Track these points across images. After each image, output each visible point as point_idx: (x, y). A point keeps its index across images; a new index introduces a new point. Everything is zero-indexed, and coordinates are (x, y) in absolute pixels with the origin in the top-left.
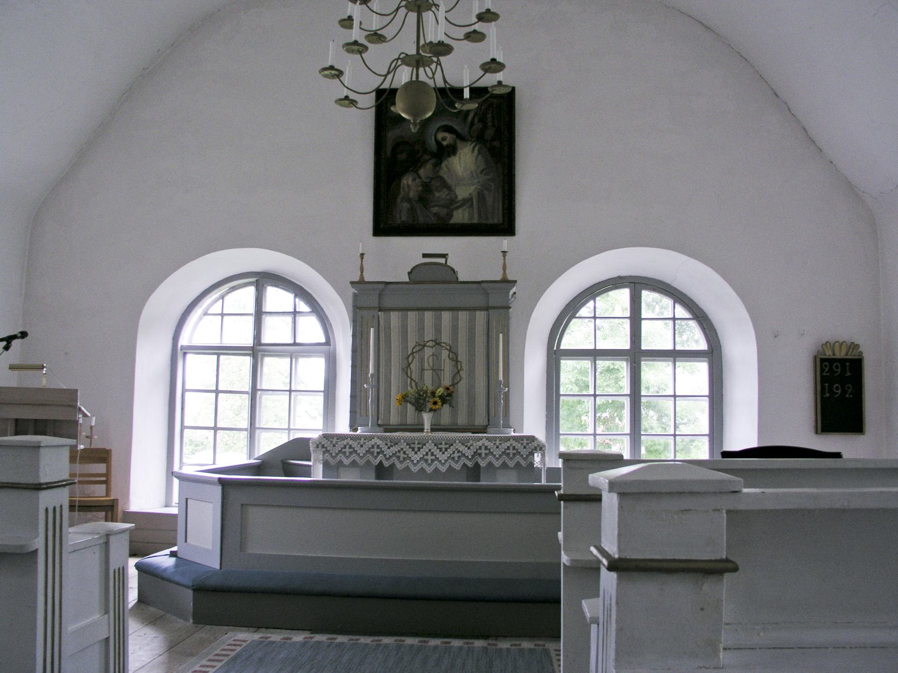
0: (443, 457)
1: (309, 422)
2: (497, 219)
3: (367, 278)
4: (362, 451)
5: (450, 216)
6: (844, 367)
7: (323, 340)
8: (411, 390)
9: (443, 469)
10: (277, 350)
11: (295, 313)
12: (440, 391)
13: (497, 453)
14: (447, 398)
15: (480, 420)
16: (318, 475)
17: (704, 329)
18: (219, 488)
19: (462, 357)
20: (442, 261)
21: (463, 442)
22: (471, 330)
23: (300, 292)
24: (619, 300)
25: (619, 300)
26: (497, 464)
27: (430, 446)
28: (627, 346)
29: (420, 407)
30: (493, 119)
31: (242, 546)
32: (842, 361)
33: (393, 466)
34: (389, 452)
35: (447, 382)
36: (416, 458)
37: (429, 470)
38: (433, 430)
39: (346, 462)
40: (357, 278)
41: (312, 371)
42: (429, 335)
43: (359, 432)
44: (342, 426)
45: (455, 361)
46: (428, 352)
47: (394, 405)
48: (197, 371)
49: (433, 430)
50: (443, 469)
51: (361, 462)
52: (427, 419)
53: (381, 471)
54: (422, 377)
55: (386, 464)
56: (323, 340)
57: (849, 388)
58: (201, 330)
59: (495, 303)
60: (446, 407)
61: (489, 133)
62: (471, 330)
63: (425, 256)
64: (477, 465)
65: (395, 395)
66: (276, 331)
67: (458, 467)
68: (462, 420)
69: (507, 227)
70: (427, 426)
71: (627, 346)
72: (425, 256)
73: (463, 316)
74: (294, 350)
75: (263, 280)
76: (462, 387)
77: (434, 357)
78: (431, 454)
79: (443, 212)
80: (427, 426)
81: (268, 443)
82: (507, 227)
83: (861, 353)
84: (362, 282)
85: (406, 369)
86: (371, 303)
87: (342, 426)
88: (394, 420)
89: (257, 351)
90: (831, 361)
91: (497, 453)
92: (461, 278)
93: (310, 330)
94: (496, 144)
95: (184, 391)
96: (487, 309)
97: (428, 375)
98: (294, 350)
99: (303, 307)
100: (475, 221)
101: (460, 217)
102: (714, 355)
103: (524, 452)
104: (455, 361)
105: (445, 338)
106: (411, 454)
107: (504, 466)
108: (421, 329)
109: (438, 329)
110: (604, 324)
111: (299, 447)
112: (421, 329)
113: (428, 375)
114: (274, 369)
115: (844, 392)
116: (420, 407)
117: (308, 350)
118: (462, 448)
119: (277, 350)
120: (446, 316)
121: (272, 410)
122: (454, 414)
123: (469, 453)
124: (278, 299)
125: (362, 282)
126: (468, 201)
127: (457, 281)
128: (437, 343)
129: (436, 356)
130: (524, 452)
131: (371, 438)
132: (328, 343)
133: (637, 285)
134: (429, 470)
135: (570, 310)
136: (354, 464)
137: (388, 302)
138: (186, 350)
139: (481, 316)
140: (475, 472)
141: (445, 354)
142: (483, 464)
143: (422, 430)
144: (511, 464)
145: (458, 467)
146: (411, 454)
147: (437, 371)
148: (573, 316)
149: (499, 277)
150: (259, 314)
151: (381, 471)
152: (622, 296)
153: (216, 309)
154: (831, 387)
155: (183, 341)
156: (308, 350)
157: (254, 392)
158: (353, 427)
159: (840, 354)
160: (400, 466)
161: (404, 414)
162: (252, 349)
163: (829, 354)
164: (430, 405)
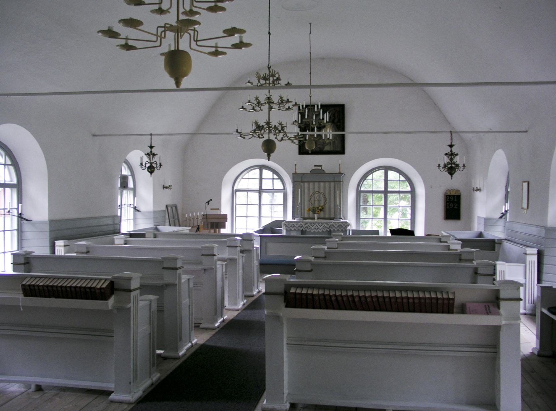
0: (320, 228)
1: (278, 214)
2: (339, 149)
3: (298, 172)
4: (297, 226)
5: (324, 148)
6: (454, 198)
7: (283, 188)
8: (311, 207)
9: (320, 231)
10: (267, 191)
11: (273, 179)
12: (320, 208)
13: (336, 227)
14: (322, 209)
15: (332, 216)
16: (284, 233)
17: (409, 184)
18: (259, 238)
19: (327, 196)
20: (320, 168)
21: (327, 223)
22: (330, 188)
23: (274, 172)
24: (380, 174)
25: (380, 174)
26: (336, 230)
27: (317, 224)
28: (383, 189)
29: (314, 212)
30: (338, 114)
31: (266, 253)
32: (454, 196)
33: (306, 230)
34: (305, 226)
35: (322, 204)
36: (312, 228)
37: (316, 231)
38: (318, 219)
39: (293, 229)
40: (294, 172)
41: (279, 197)
42: (317, 190)
43: (295, 220)
44: (290, 218)
45: (325, 198)
46: (316, 195)
47: (306, 212)
48: (241, 197)
49: (318, 219)
50: (320, 231)
51: (297, 229)
52: (316, 216)
53: (303, 232)
54: (315, 203)
55: (304, 230)
56: (283, 188)
57: (456, 205)
58: (241, 184)
59: (337, 180)
60: (322, 212)
61: (336, 120)
62: (330, 188)
63: (315, 166)
64: (330, 230)
65: (307, 209)
66: (267, 185)
67: (325, 231)
68: (327, 216)
69: (342, 151)
70: (316, 218)
71: (383, 189)
72: (315, 166)
73: (327, 184)
74: (273, 191)
75: (261, 168)
76: (327, 206)
77: (318, 196)
78: (317, 225)
79: (322, 147)
80: (316, 218)
81: (266, 222)
82: (342, 151)
83: (460, 193)
84: (296, 173)
85: (310, 200)
86: (299, 180)
87: (290, 218)
88: (306, 216)
89: (260, 191)
90: (450, 196)
91: (336, 227)
92: (326, 172)
93: (278, 185)
94: (339, 124)
95: (236, 204)
96: (334, 182)
97: (316, 202)
98: (273, 191)
99: (275, 177)
100: (332, 150)
101: (327, 148)
102: (413, 192)
103: (344, 226)
104: (325, 198)
105: (322, 191)
106: (311, 227)
107: (338, 230)
108: (314, 188)
109: (319, 188)
110: (376, 182)
111: (277, 223)
112: (314, 188)
113: (316, 202)
114: (266, 197)
115: (454, 206)
116: (314, 212)
117: (278, 190)
118: (326, 225)
119: (267, 191)
120: (322, 184)
121: (266, 210)
122: (325, 214)
123: (328, 227)
124: (267, 174)
125: (296, 173)
126: (329, 143)
127: (325, 173)
128: (319, 192)
129: (319, 196)
130: (344, 226)
131: (298, 222)
132: (284, 189)
133: (387, 169)
134: (316, 231)
135: (364, 177)
136: (295, 230)
137: (304, 180)
138: (237, 191)
139: (332, 184)
140: (330, 232)
141: (322, 195)
142: (332, 230)
143: (314, 219)
144: (340, 230)
145: (325, 231)
146: (311, 227)
147: (319, 201)
148: (365, 179)
149: (338, 172)
150: (261, 179)
151: (303, 232)
152: (381, 173)
153: (246, 176)
154: (449, 206)
155: (235, 188)
156: (278, 190)
157: (260, 205)
158: (294, 217)
159: (453, 193)
160: (308, 230)
161: (309, 214)
162: (259, 190)
163: (449, 193)
164: (317, 212)
